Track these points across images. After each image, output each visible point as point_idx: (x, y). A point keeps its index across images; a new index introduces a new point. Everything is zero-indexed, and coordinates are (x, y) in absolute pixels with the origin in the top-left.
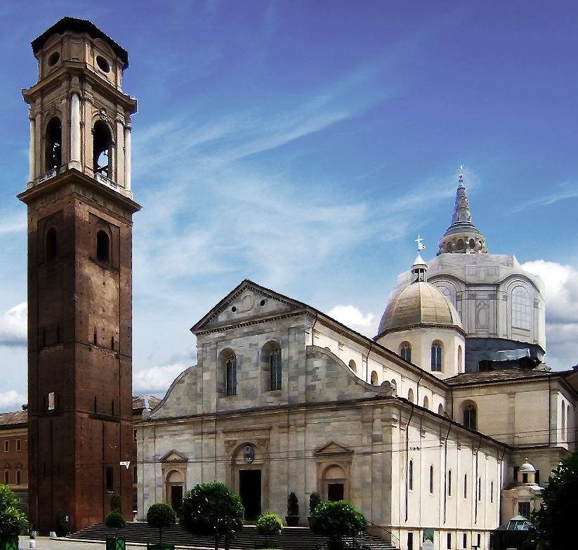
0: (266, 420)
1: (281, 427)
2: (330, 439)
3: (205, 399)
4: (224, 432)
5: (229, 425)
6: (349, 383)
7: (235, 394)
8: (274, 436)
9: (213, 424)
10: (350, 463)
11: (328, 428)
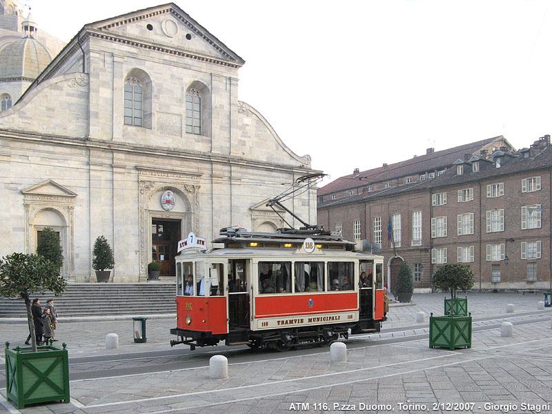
0: (193, 164)
4: (137, 168)
5: (145, 161)
6: (277, 149)
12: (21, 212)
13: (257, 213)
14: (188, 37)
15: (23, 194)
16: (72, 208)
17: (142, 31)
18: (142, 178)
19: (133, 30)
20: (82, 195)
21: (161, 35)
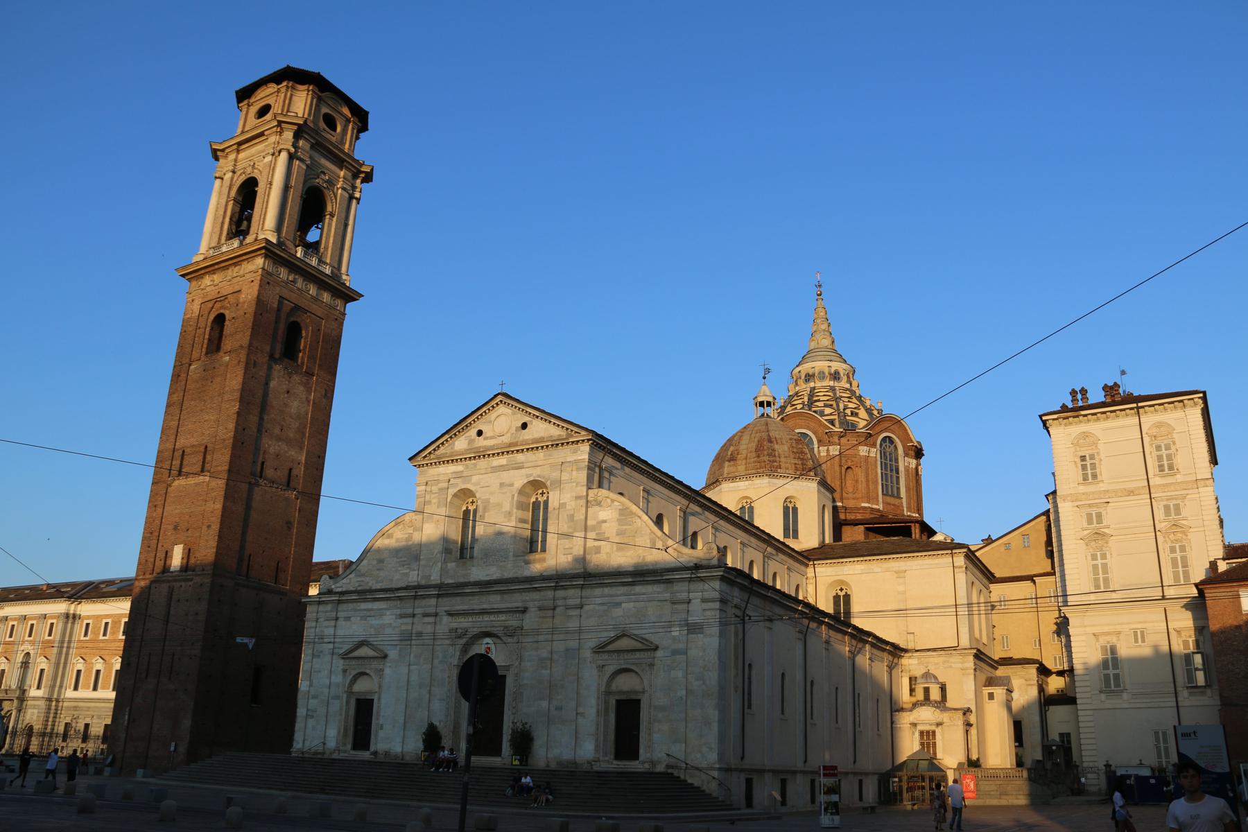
0: (517, 596)
1: (540, 609)
2: (619, 633)
3: (422, 563)
4: (450, 614)
5: (458, 604)
7: (472, 557)
8: (530, 621)
9: (433, 601)
10: (651, 665)
11: (617, 612)
12: (338, 678)
13: (606, 656)
14: (524, 426)
15: (346, 656)
16: (382, 670)
17: (471, 441)
18: (454, 625)
19: (460, 444)
20: (393, 654)
21: (492, 438)
